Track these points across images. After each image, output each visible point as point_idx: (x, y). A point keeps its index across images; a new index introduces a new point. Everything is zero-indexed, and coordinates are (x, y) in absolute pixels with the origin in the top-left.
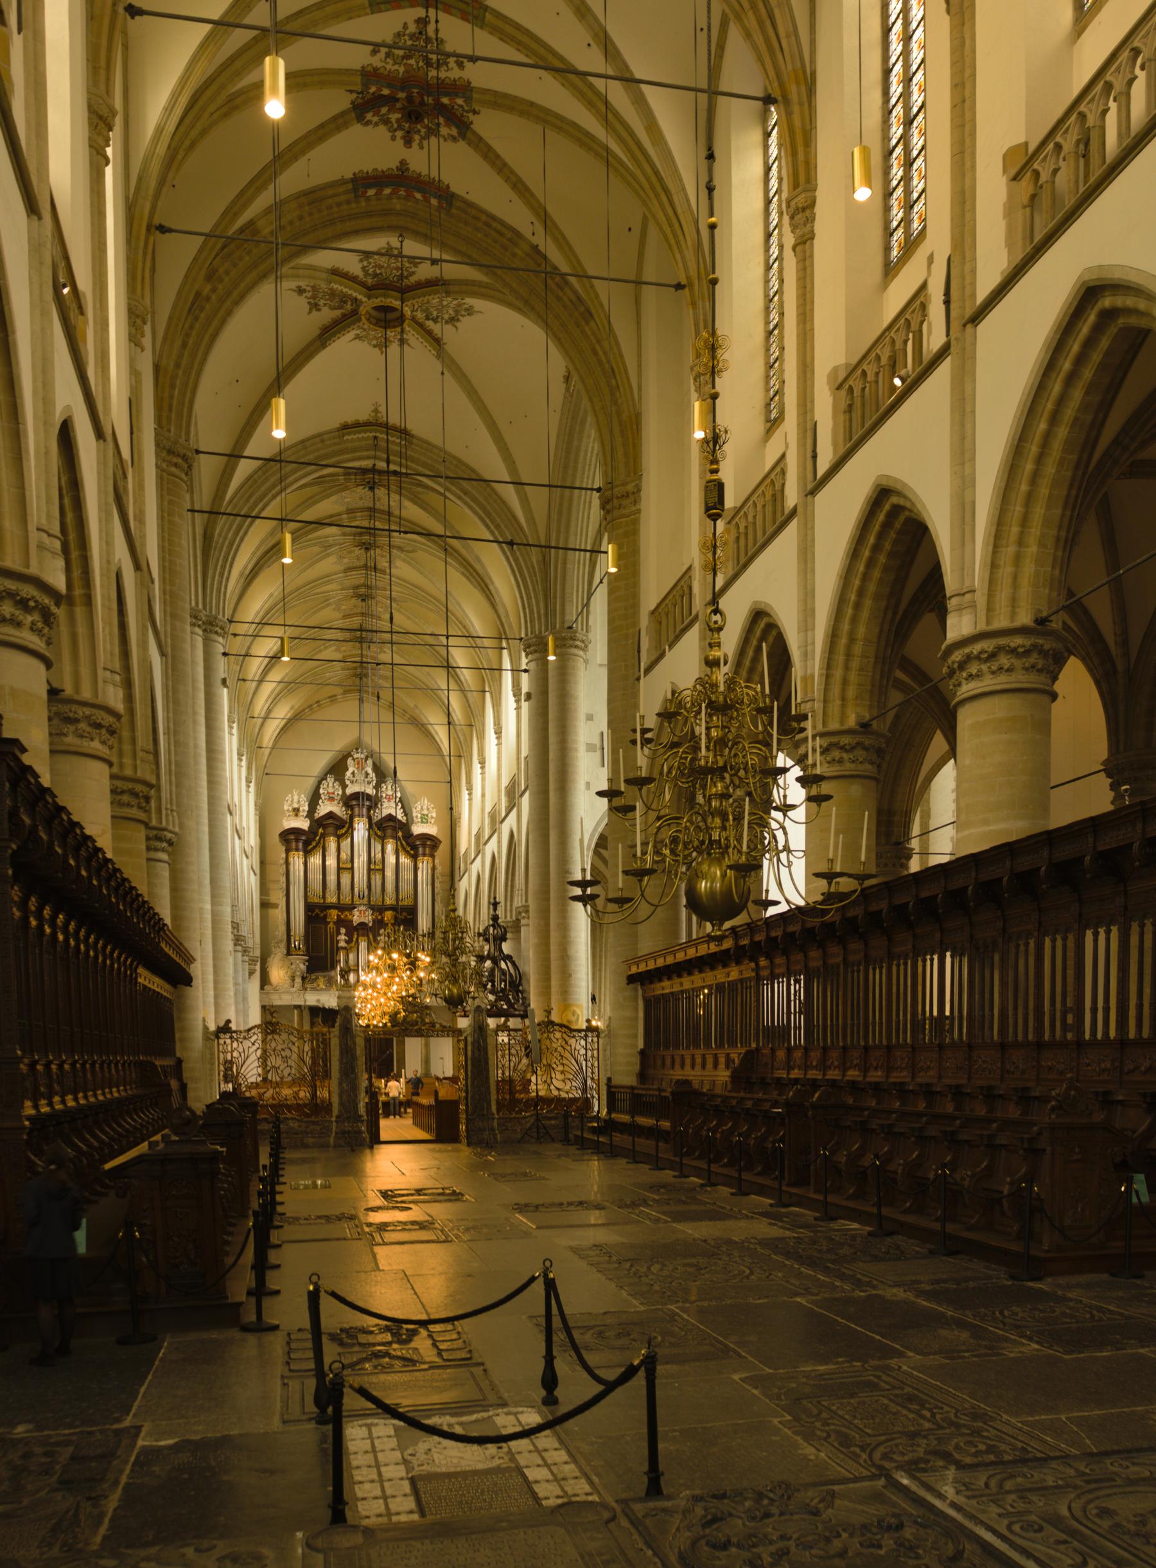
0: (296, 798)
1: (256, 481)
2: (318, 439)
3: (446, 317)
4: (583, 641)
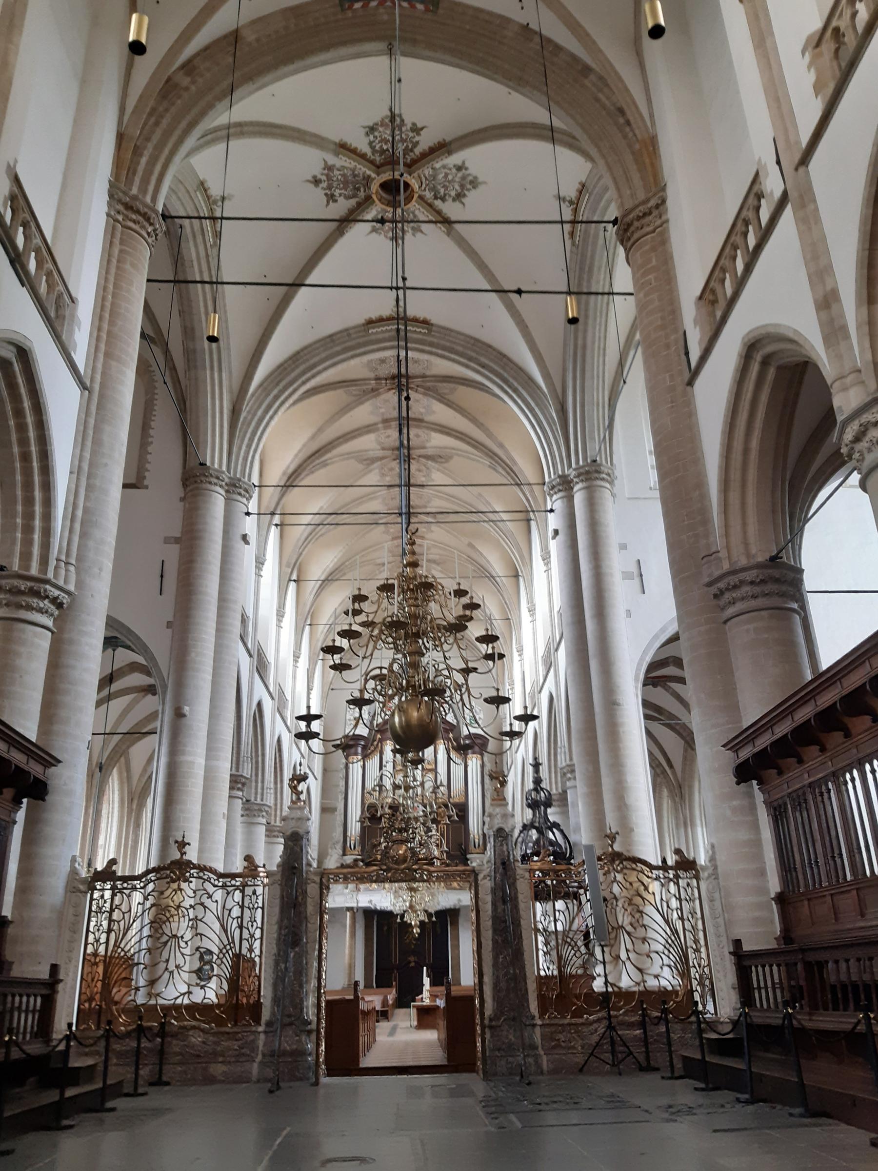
1: (285, 369)
2: (345, 334)
3: (453, 193)
4: (608, 475)
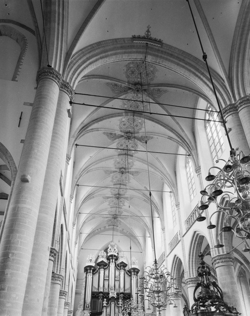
0: (91, 256)
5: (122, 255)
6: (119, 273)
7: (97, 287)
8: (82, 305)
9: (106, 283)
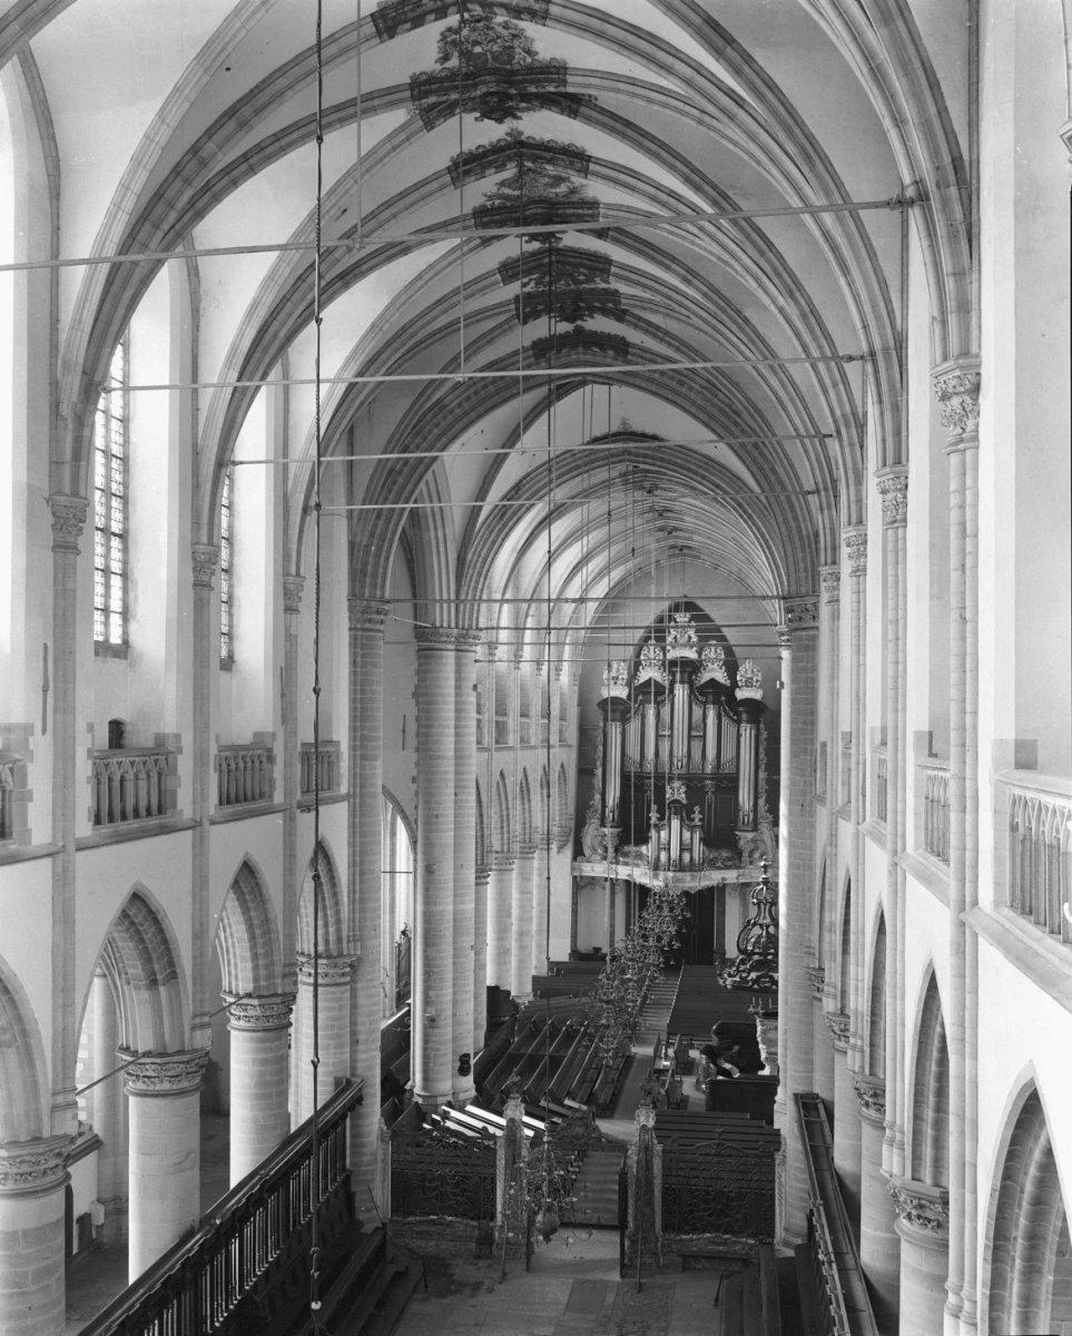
5: (712, 655)
6: (704, 713)
7: (637, 757)
8: (596, 811)
9: (665, 745)
